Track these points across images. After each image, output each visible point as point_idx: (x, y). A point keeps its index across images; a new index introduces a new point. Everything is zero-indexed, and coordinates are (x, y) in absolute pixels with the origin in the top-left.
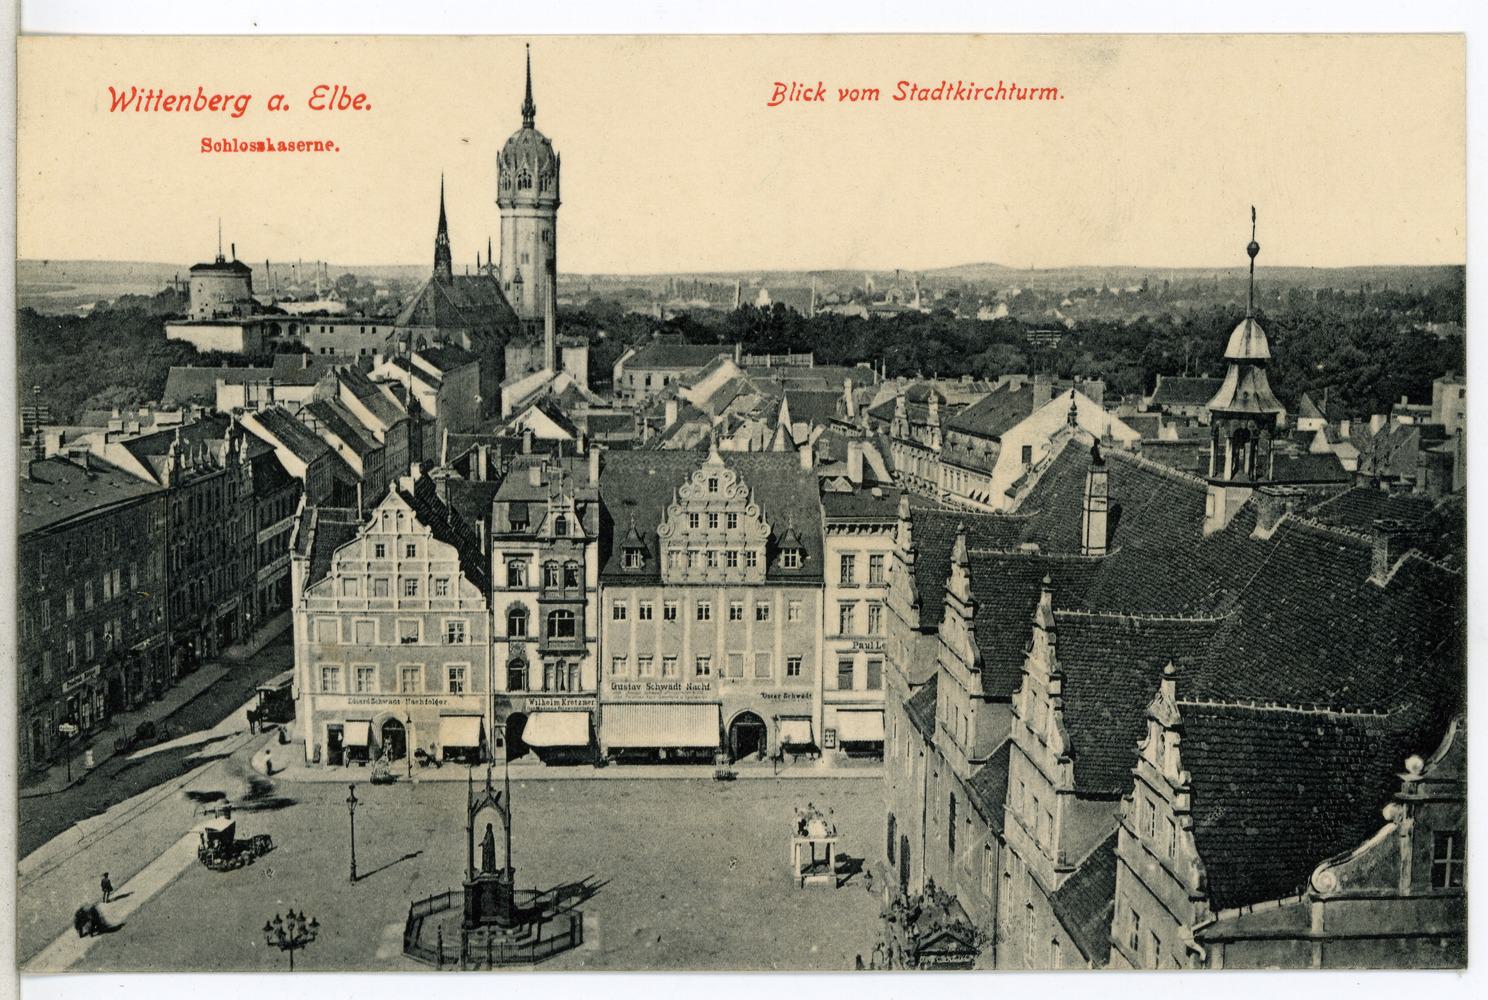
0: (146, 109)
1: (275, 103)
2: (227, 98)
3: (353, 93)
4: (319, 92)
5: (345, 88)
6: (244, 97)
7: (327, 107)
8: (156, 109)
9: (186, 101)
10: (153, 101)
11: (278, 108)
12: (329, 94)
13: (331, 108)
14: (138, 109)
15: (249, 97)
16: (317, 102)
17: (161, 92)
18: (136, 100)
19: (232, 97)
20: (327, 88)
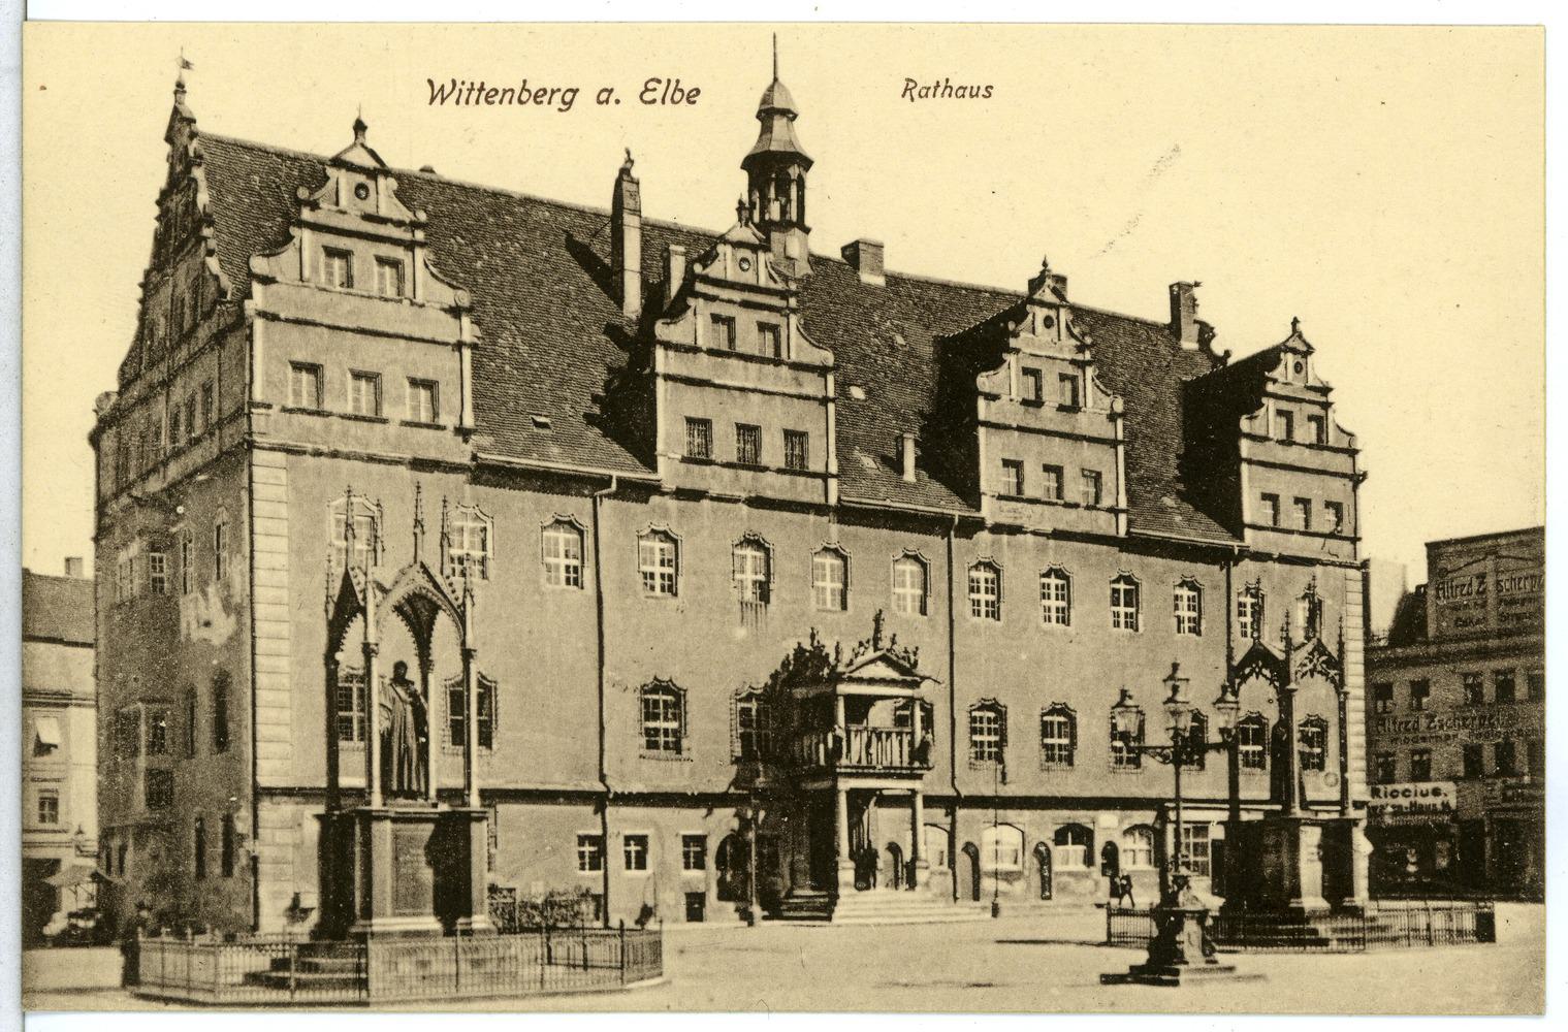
0: (467, 102)
1: (604, 96)
2: (553, 92)
3: (686, 86)
4: (651, 86)
5: (678, 81)
6: (605, 90)
7: (659, 101)
8: (477, 102)
9: (509, 95)
10: (475, 94)
11: (607, 101)
12: (661, 88)
13: (663, 102)
14: (458, 102)
15: (578, 90)
16: (648, 96)
17: (483, 84)
18: (456, 92)
19: (559, 90)
20: (659, 81)
